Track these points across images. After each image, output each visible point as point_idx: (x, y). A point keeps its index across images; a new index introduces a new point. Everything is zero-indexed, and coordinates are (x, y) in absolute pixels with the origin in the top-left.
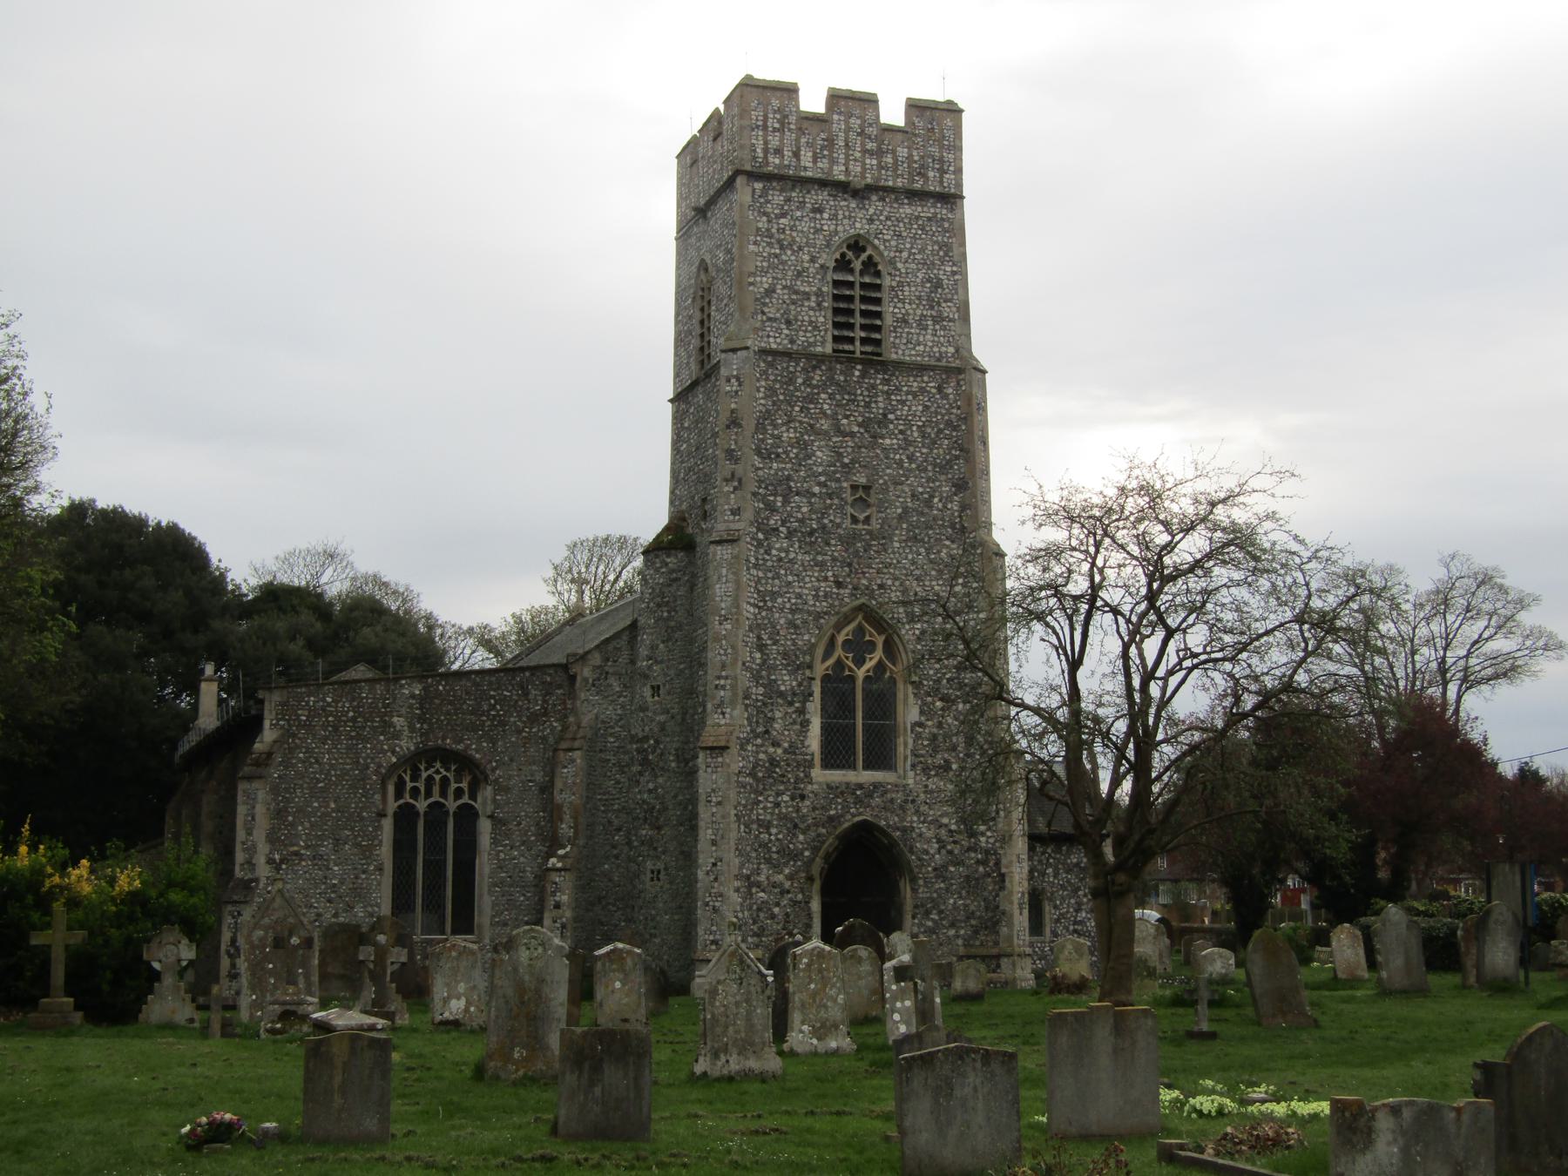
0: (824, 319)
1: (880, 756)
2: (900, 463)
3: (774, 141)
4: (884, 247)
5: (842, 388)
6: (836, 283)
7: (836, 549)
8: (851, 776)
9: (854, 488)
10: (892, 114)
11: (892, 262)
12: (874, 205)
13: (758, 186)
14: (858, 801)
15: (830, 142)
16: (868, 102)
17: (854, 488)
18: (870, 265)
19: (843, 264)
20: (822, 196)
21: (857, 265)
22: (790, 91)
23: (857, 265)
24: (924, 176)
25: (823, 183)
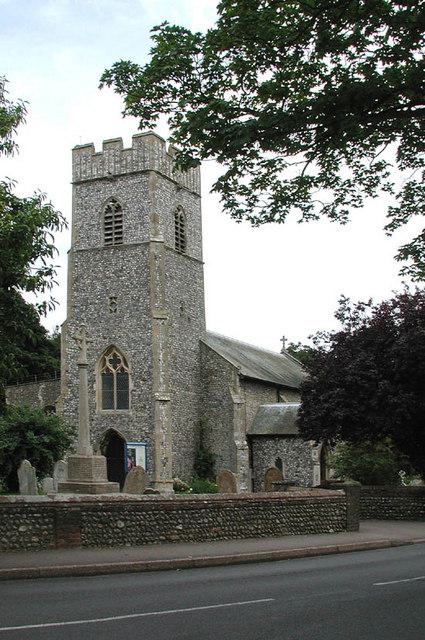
0: (101, 234)
1: (123, 403)
2: (127, 286)
3: (83, 168)
4: (121, 201)
5: (107, 260)
6: (106, 218)
7: (103, 324)
8: (110, 411)
9: (111, 298)
10: (128, 144)
11: (125, 205)
12: (119, 183)
13: (78, 187)
14: (112, 421)
15: (103, 162)
16: (119, 141)
17: (111, 298)
18: (118, 208)
19: (109, 210)
20: (100, 185)
21: (113, 208)
22: (90, 146)
23: (113, 208)
24: (137, 165)
25: (100, 180)
